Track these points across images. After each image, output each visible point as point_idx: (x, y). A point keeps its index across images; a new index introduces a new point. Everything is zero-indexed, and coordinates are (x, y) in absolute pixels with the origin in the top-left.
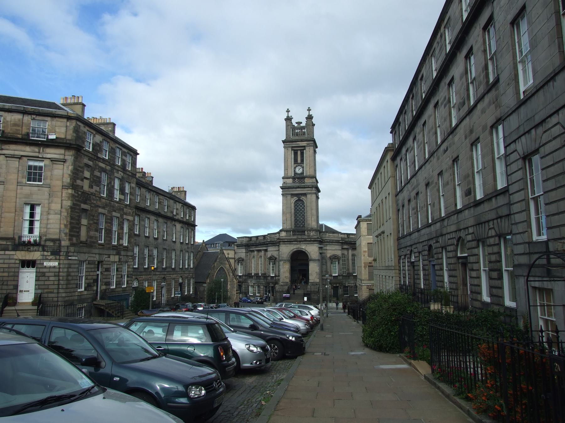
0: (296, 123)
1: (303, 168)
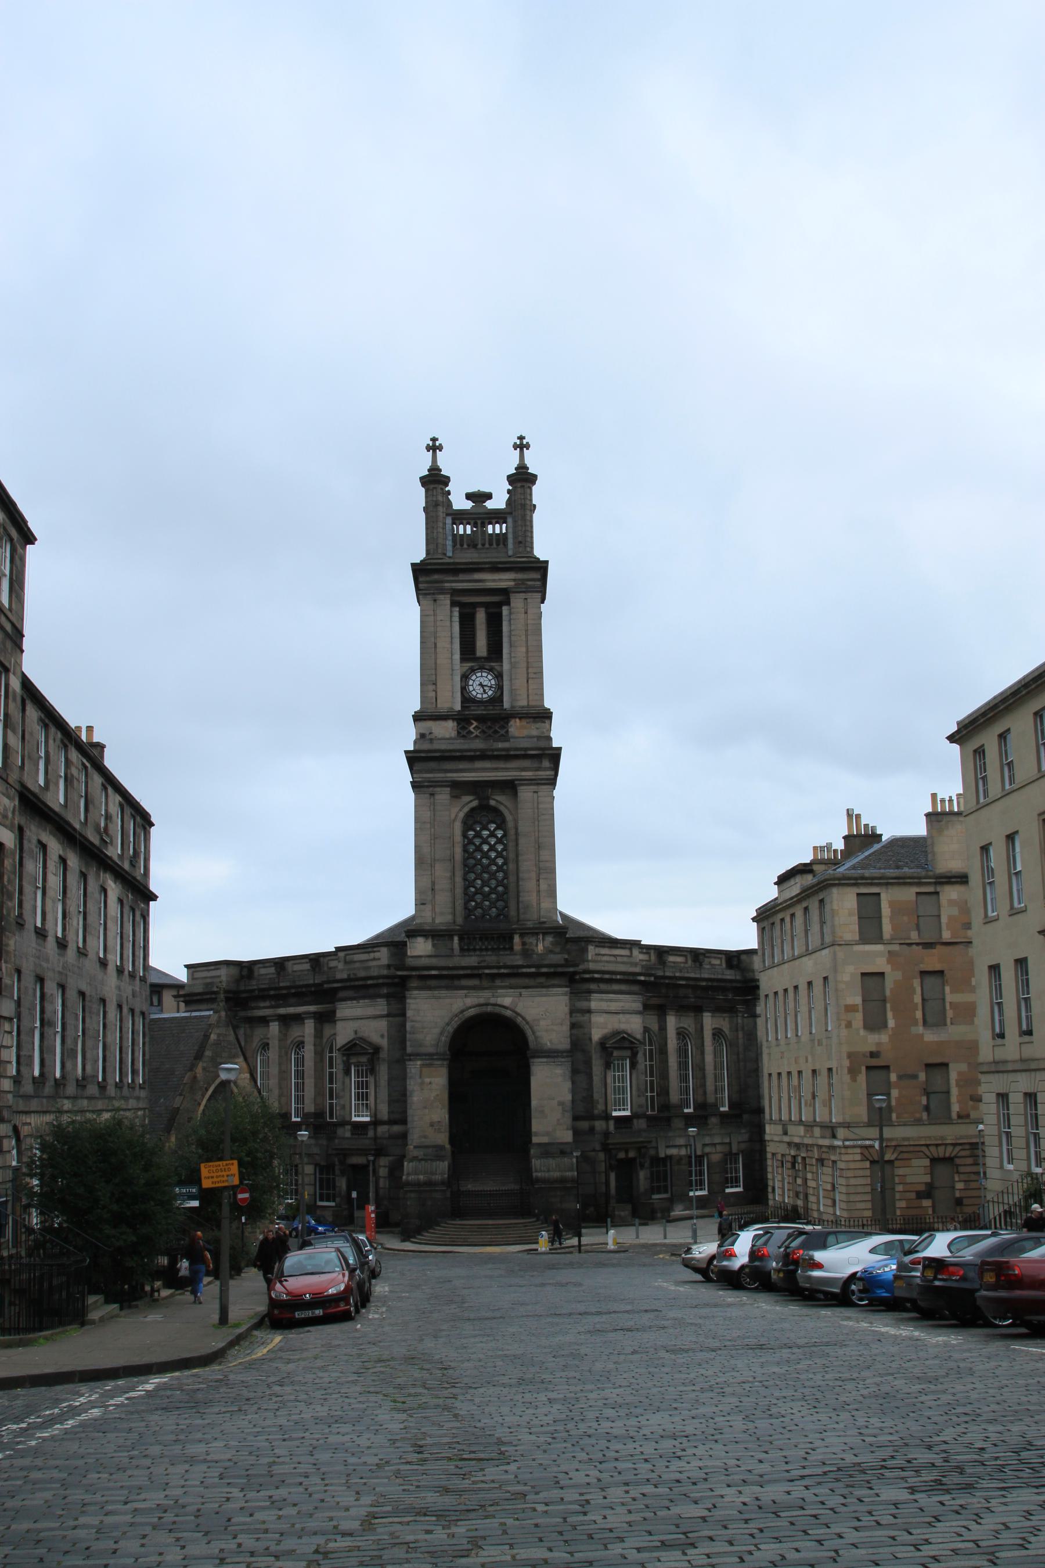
0: (469, 496)
1: (499, 676)
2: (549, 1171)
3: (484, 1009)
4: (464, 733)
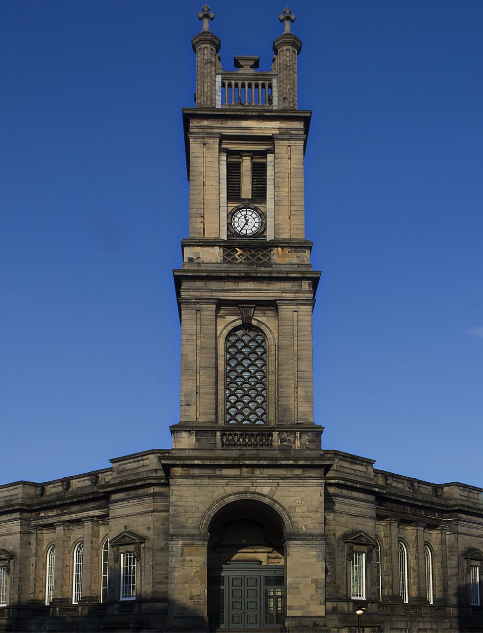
3: (243, 497)
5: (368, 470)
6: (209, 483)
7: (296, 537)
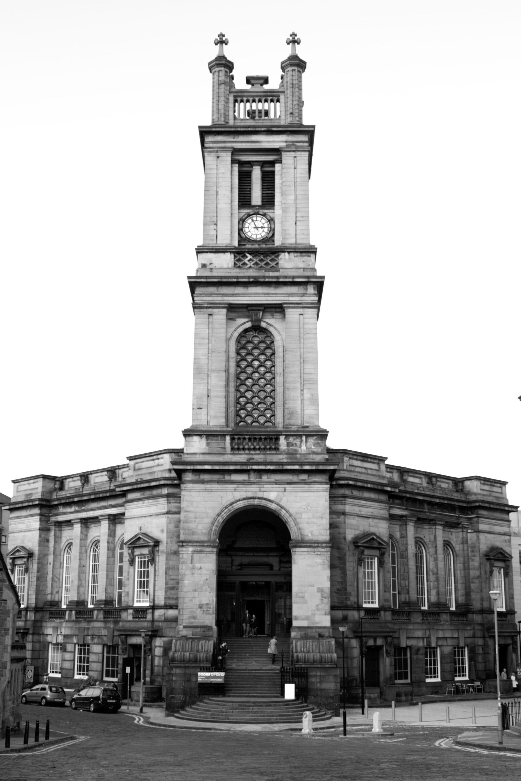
1: (271, 220)
2: (308, 652)
3: (251, 502)
4: (240, 264)
5: (380, 468)
6: (219, 488)
7: (302, 545)
